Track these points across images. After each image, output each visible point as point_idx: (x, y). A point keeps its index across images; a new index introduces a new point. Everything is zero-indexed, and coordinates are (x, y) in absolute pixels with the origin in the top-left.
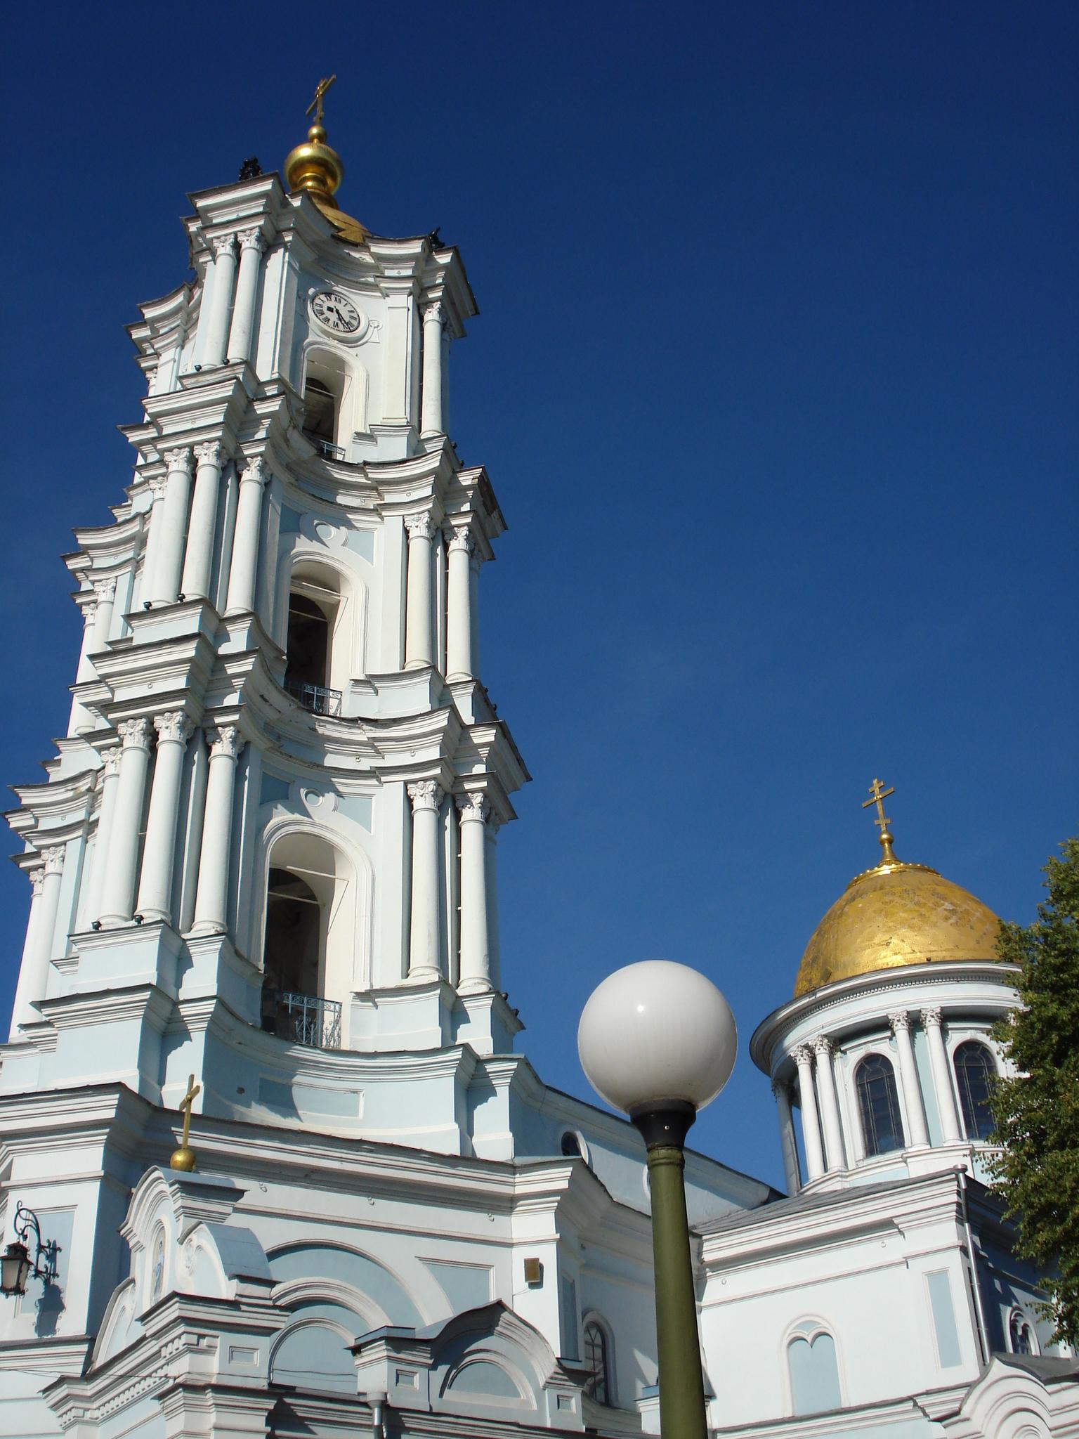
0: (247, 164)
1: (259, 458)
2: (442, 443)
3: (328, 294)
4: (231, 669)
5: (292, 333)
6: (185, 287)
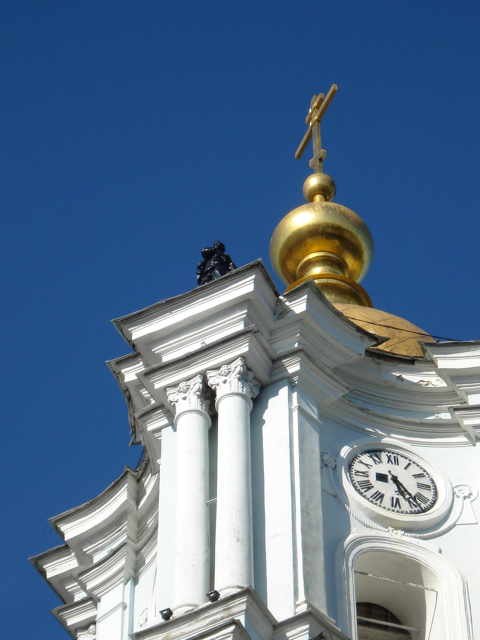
5: (321, 528)
6: (129, 476)
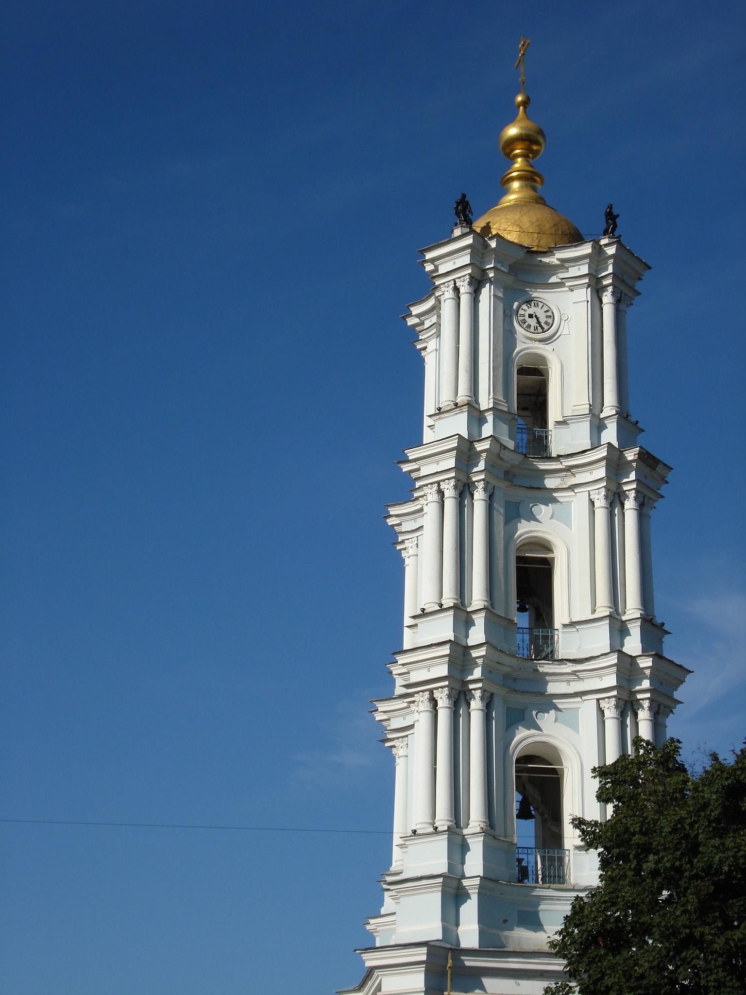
0: (458, 204)
1: (482, 482)
2: (616, 420)
3: (529, 302)
4: (475, 654)
